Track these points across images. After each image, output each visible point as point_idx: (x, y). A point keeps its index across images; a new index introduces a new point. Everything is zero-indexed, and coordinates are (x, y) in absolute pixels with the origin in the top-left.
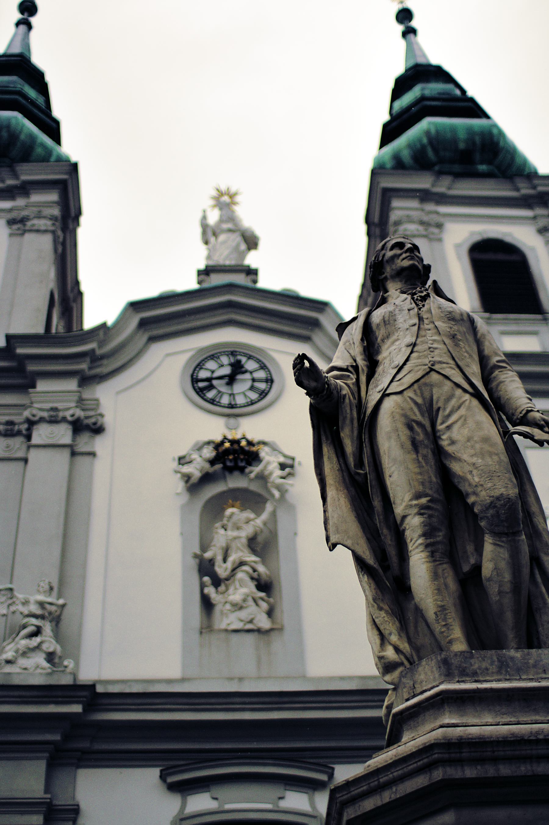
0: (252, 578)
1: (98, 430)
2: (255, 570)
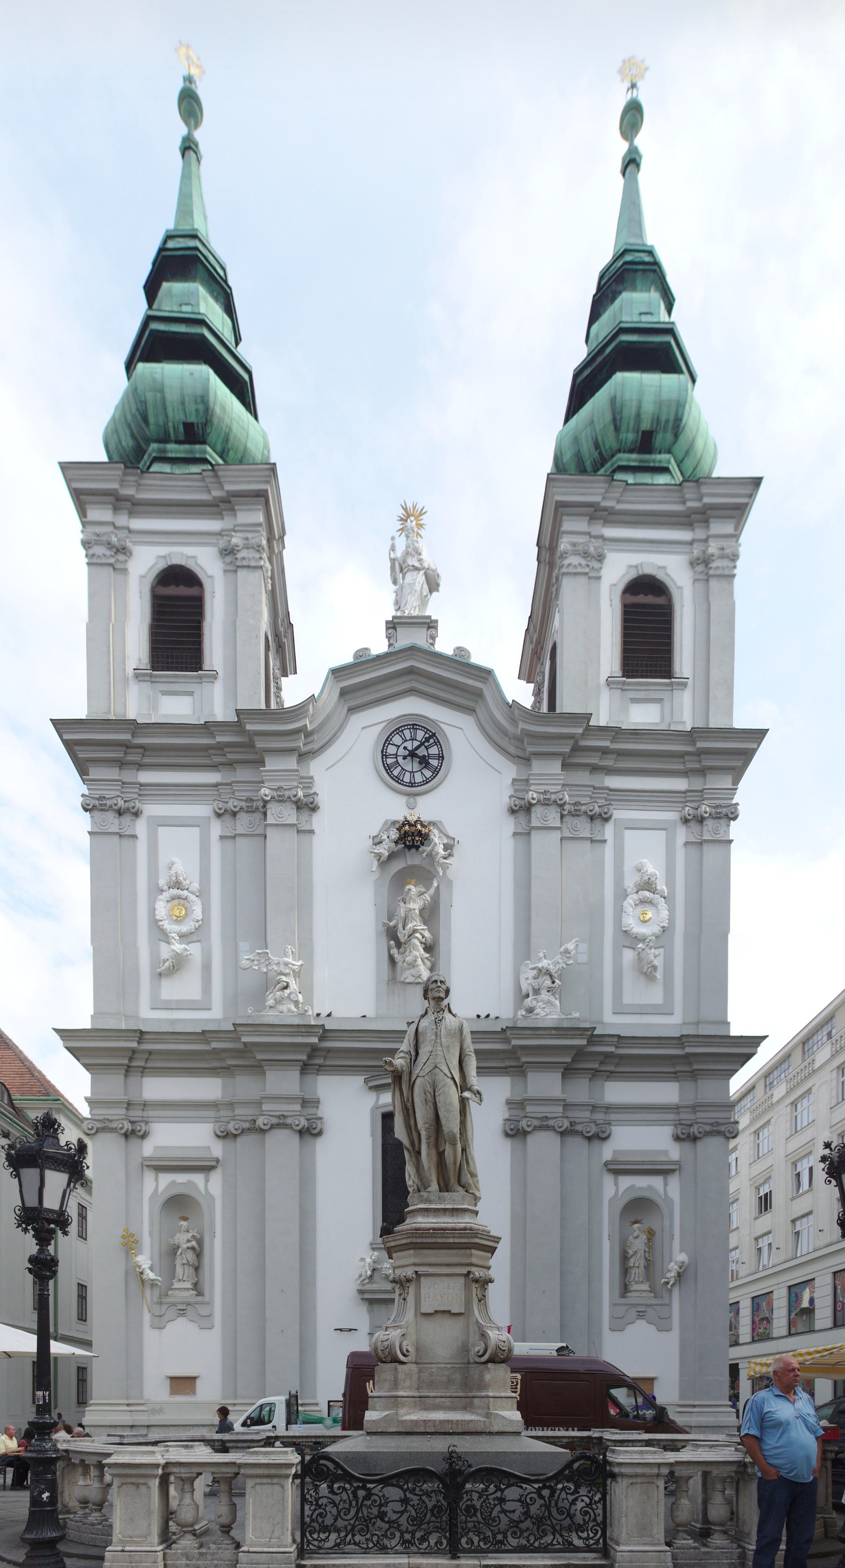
0: (421, 943)
1: (313, 808)
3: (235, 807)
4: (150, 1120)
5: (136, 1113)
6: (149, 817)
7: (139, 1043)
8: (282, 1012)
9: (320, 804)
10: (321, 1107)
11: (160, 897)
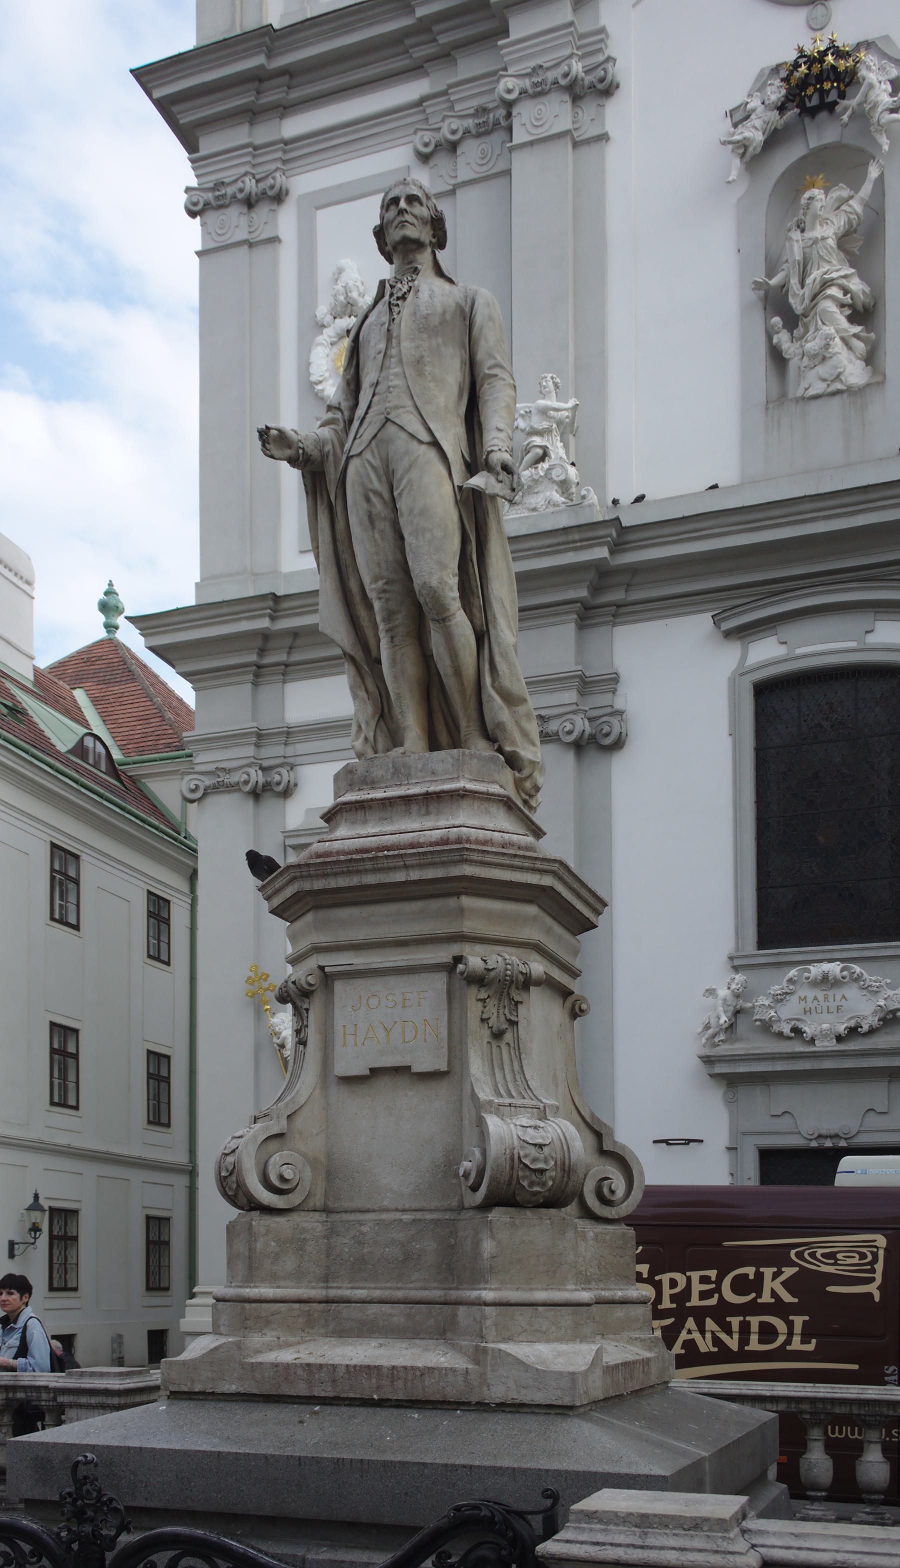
0: (842, 306)
2: (846, 291)
3: (454, 132)
4: (299, 760)
5: (272, 752)
6: (300, 197)
7: (273, 619)
8: (534, 509)
9: (621, 78)
10: (621, 689)
11: (320, 339)
